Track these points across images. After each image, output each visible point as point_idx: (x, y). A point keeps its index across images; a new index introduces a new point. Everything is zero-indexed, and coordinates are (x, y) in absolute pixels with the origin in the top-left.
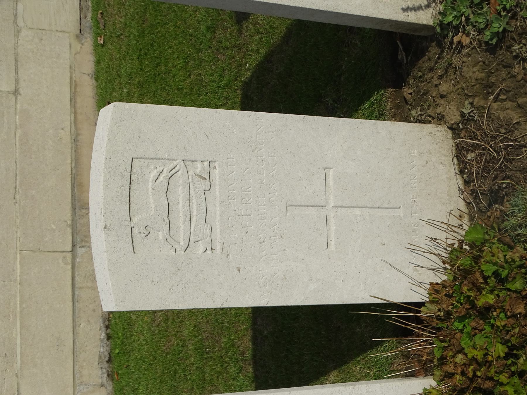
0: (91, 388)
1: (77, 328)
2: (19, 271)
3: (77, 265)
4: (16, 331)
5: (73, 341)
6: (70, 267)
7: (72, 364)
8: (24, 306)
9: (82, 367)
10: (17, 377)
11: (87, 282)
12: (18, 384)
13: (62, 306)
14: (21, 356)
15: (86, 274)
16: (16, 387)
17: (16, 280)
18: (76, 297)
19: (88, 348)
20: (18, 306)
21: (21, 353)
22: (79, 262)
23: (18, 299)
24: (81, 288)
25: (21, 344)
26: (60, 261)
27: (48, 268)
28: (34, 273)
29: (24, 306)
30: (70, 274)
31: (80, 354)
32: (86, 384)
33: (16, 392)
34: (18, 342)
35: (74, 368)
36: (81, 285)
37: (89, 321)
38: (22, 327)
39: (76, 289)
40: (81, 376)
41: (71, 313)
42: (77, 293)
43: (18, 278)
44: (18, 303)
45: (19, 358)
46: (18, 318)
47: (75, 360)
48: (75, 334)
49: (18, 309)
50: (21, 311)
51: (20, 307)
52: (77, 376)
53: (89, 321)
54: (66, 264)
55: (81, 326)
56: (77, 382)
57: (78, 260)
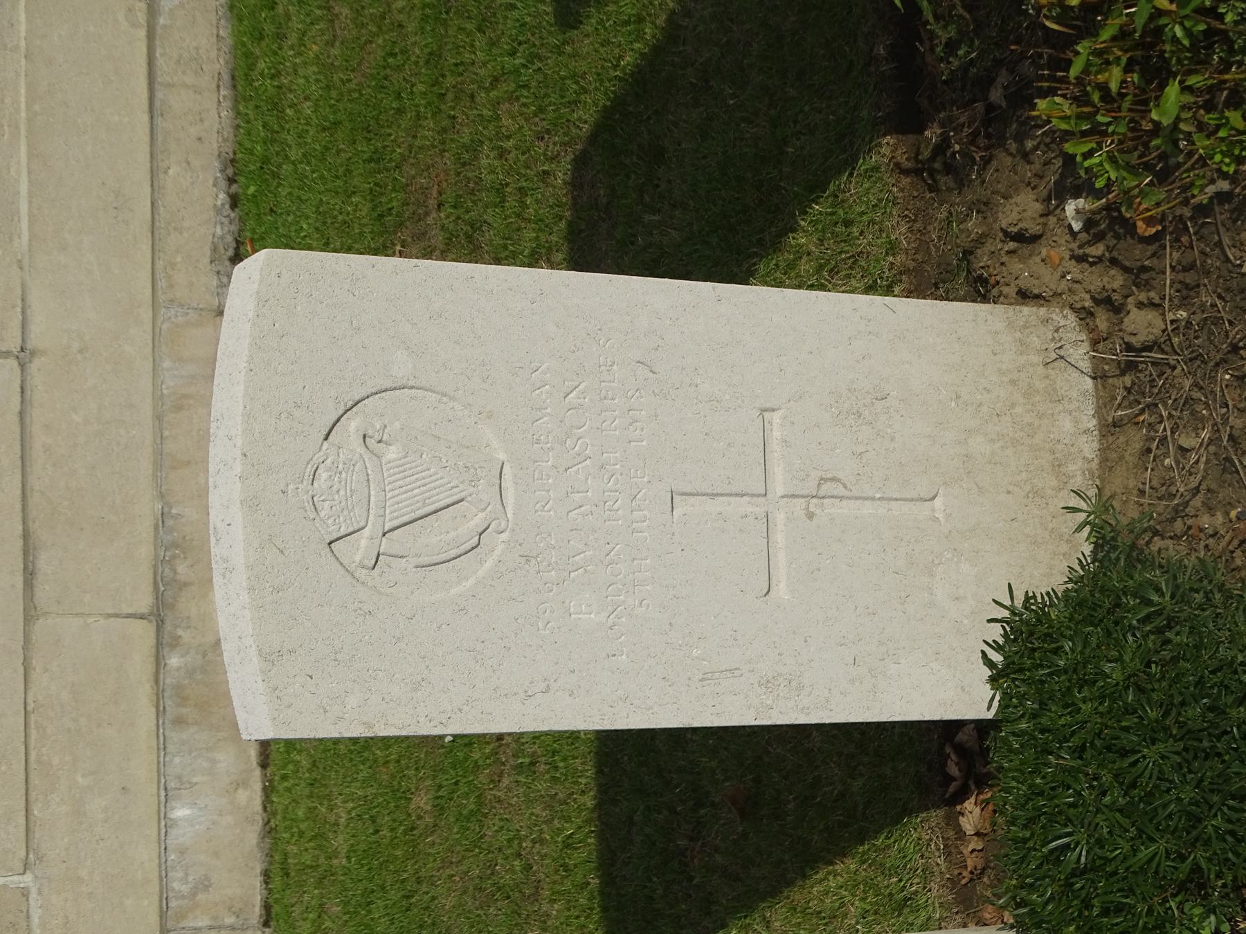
0: (193, 315)
1: (161, 176)
2: (23, 28)
3: (159, 31)
4: (19, 162)
5: (152, 204)
6: (142, 33)
7: (149, 255)
8: (37, 108)
9: (173, 265)
10: (21, 268)
11: (184, 73)
12: (23, 285)
13: (126, 120)
14: (29, 221)
15: (180, 56)
16: (19, 292)
17: (17, 47)
18: (157, 104)
19: (186, 224)
20: (23, 106)
21: (31, 215)
22: (165, 26)
23: (23, 91)
24: (171, 85)
25: (31, 195)
26: (121, 17)
27: (92, 29)
28: (60, 36)
29: (37, 108)
30: (145, 50)
31: (169, 234)
32: (182, 306)
33: (19, 302)
34: (24, 188)
35: (153, 263)
36: (168, 79)
37: (188, 163)
38: (31, 156)
39: (157, 86)
40: (171, 286)
41: (147, 139)
42: (159, 95)
43: (23, 43)
44: (23, 99)
45: (24, 225)
46: (23, 132)
47: (157, 248)
48: (156, 188)
49: (23, 115)
50: (30, 120)
51: (28, 109)
52: (162, 284)
53: (188, 163)
54: (134, 25)
55: (171, 172)
56: (162, 298)
57: (162, 21)
